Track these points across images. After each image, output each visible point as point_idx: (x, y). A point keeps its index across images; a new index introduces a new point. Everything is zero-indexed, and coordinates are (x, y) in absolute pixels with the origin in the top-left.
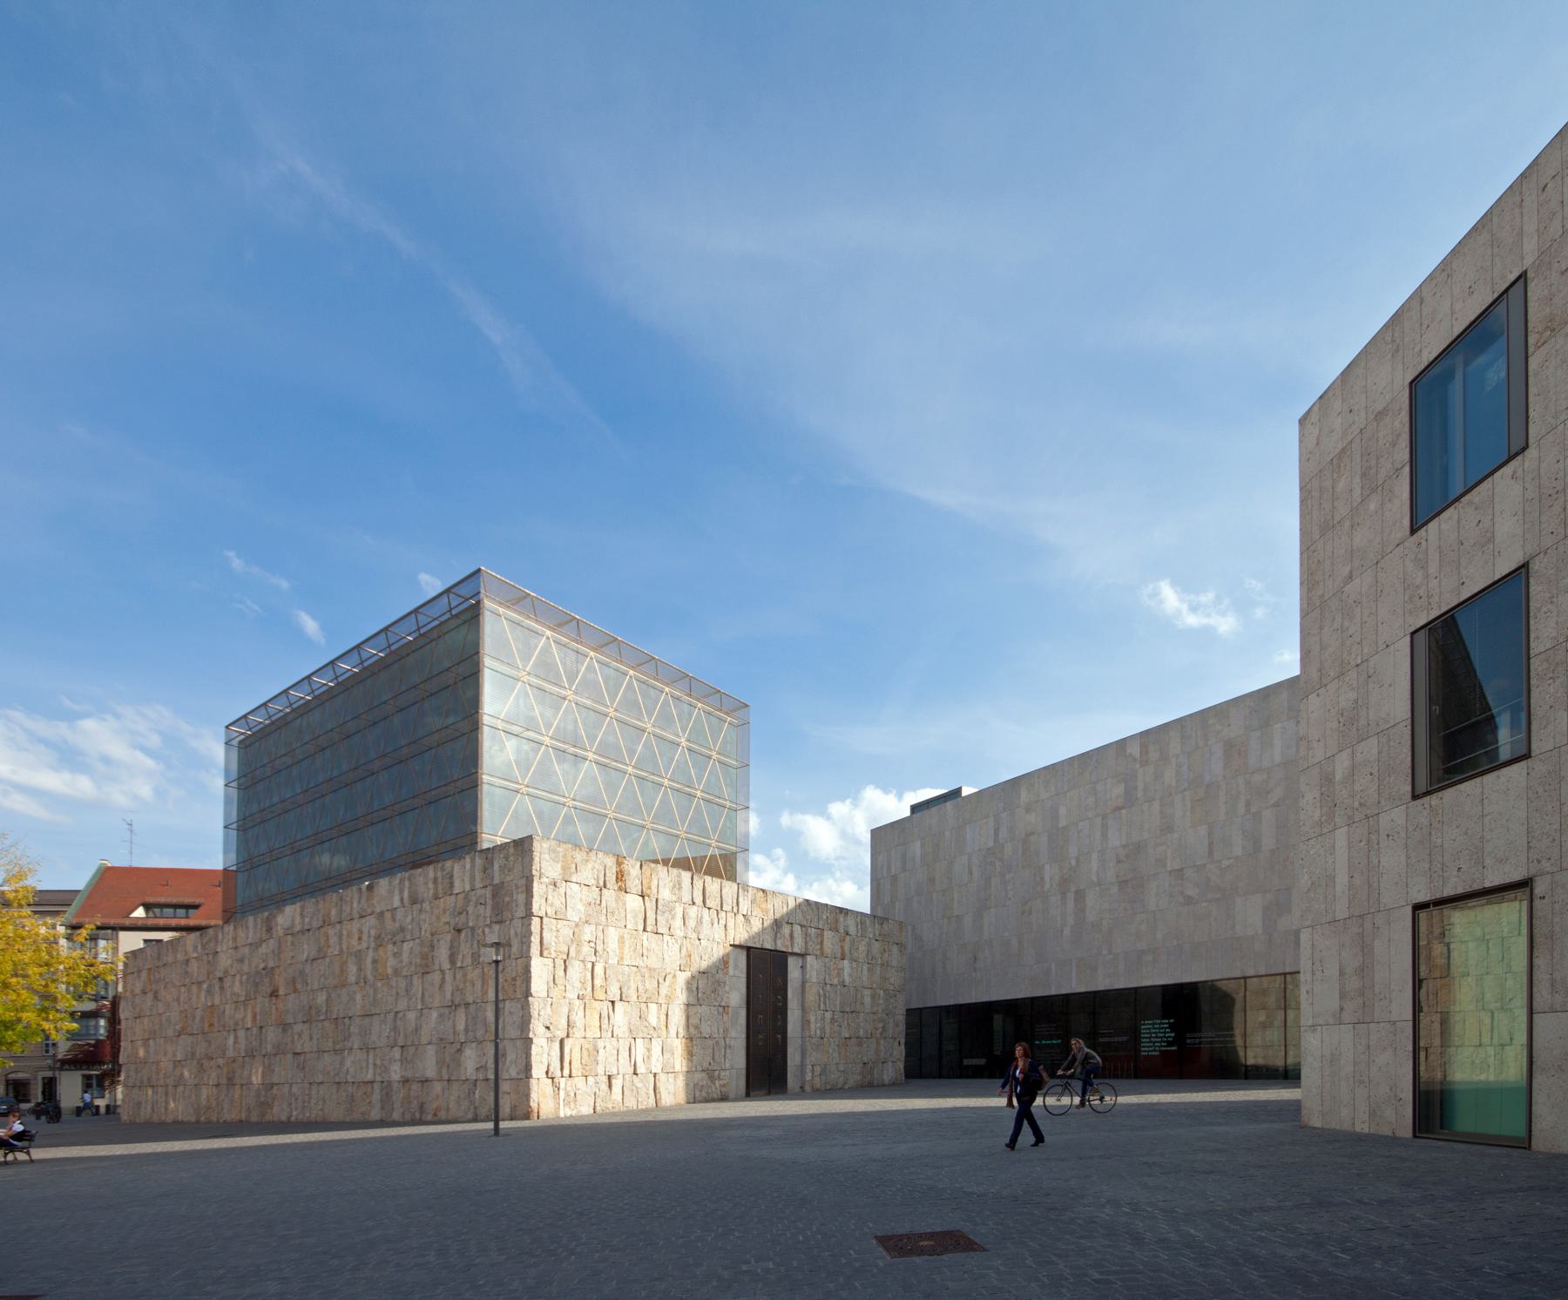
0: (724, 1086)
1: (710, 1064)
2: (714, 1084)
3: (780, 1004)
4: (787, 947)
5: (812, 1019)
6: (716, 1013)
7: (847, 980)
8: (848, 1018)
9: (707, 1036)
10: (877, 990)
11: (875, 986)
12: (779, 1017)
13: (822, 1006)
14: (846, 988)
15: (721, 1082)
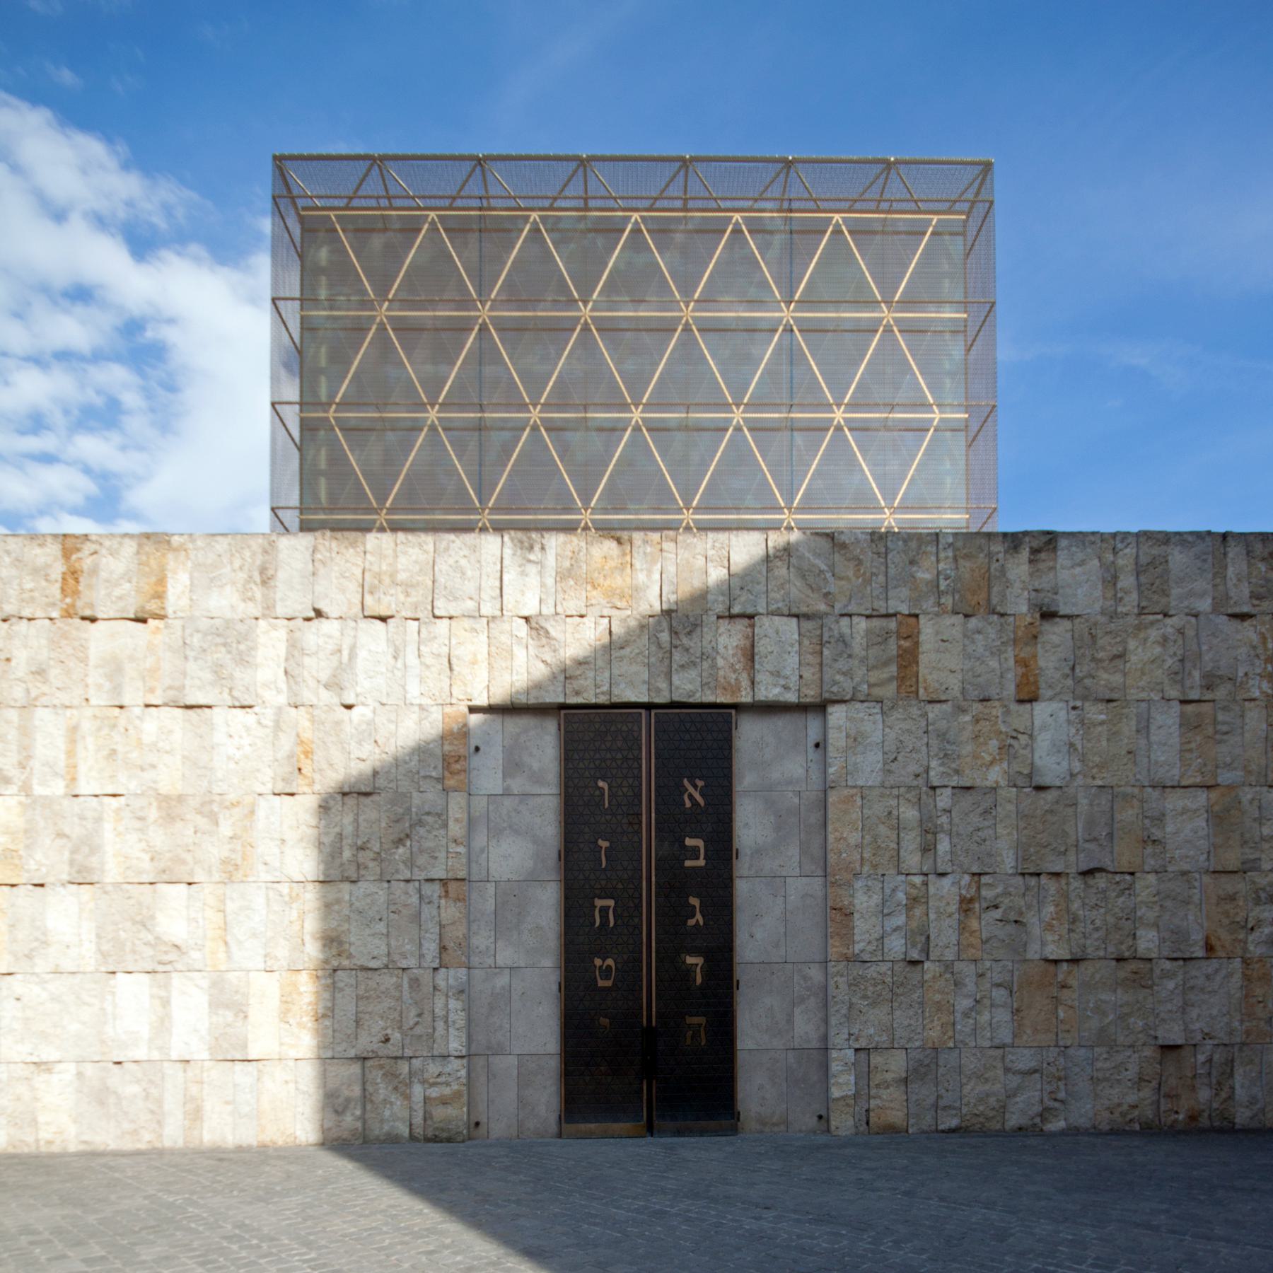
0: (444, 1102)
1: (387, 1040)
2: (408, 1097)
3: (701, 862)
4: (736, 689)
5: (863, 901)
6: (414, 899)
7: (1052, 766)
8: (1066, 896)
9: (373, 964)
10: (1247, 795)
11: (1225, 777)
12: (694, 901)
13: (912, 860)
14: (1050, 796)
15: (434, 1092)
